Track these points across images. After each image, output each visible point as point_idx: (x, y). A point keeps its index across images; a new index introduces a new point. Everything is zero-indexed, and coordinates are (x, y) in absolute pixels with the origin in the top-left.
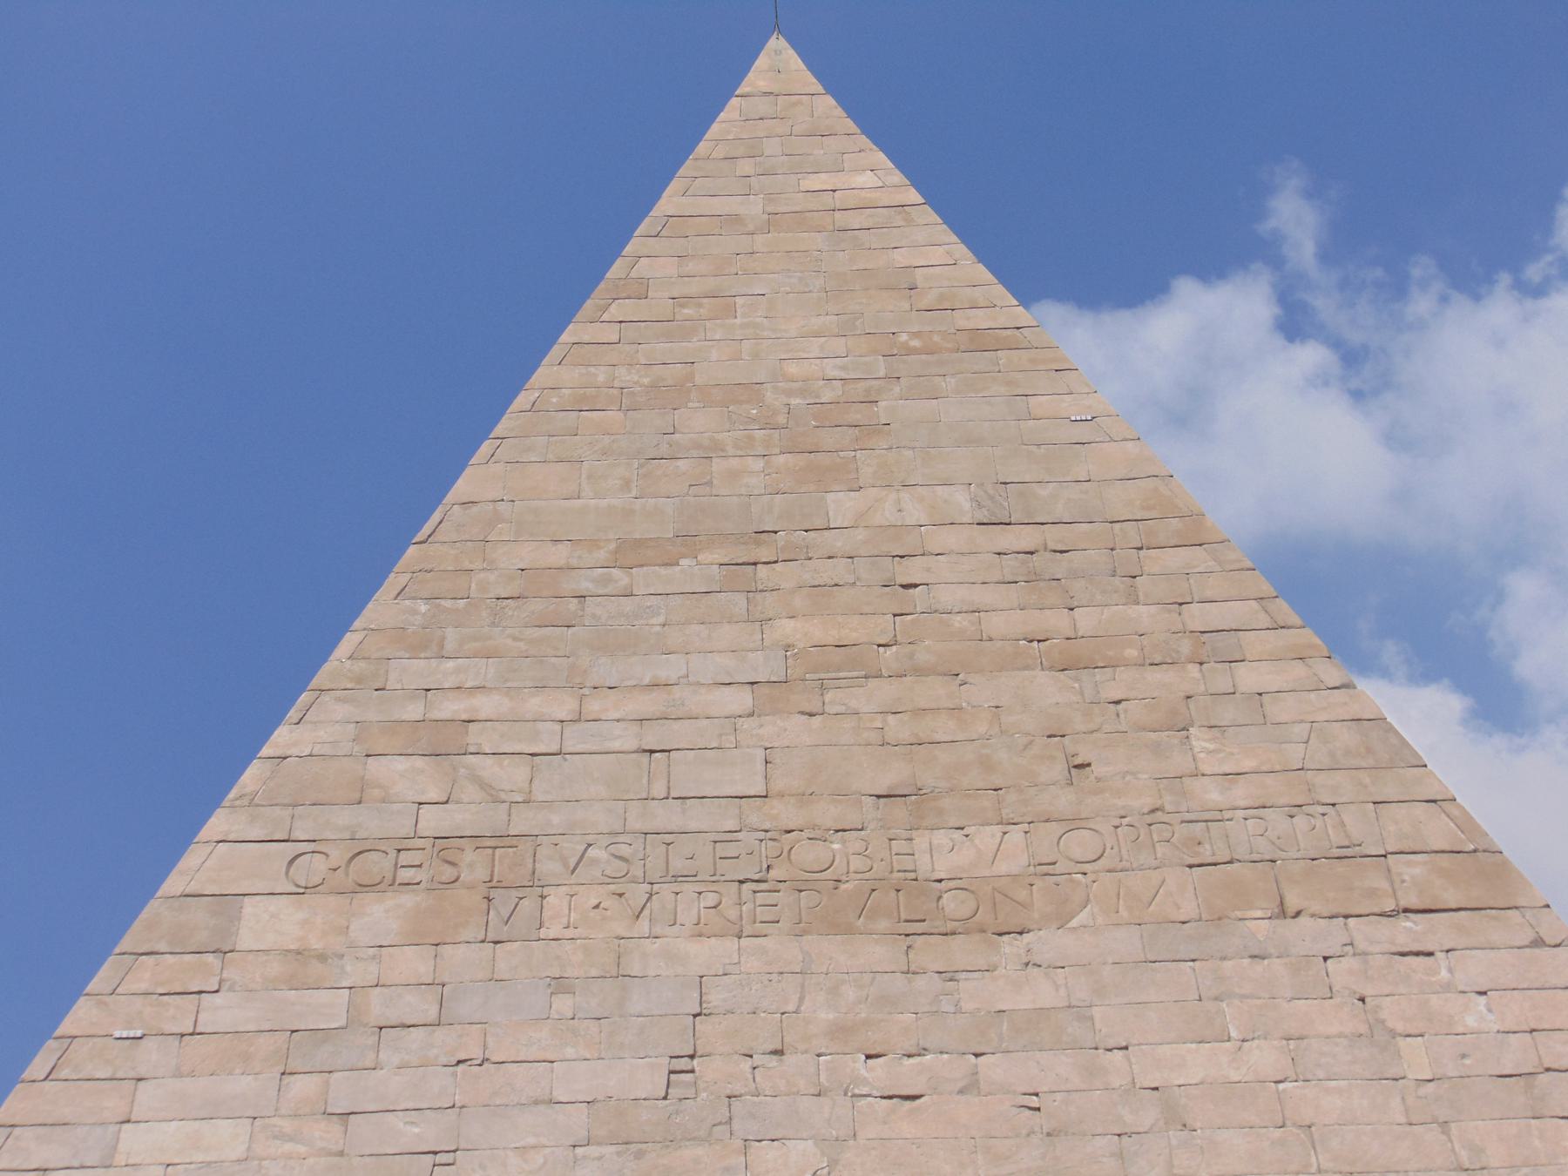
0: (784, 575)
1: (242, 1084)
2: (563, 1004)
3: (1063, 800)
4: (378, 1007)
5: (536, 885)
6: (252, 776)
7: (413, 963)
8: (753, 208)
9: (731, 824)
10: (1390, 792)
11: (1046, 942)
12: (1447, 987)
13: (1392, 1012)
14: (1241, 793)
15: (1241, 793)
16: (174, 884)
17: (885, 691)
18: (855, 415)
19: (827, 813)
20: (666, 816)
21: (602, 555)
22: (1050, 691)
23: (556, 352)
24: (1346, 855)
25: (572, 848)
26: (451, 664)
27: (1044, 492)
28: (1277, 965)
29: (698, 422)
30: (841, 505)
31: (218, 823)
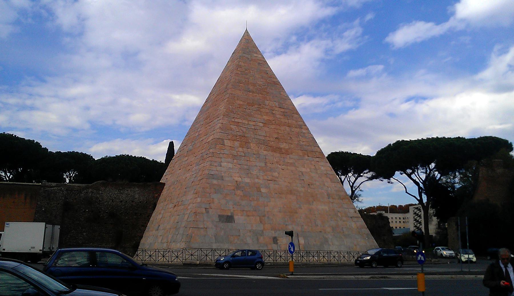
8: (249, 57)
11: (291, 156)
20: (258, 137)
22: (287, 129)
30: (267, 102)
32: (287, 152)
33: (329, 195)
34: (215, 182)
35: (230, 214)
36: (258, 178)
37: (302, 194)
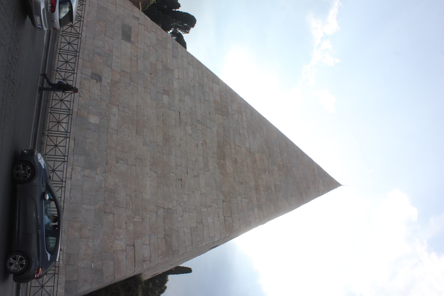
2: (208, 113)
22: (252, 184)
32: (222, 167)
35: (132, 39)
36: (181, 100)
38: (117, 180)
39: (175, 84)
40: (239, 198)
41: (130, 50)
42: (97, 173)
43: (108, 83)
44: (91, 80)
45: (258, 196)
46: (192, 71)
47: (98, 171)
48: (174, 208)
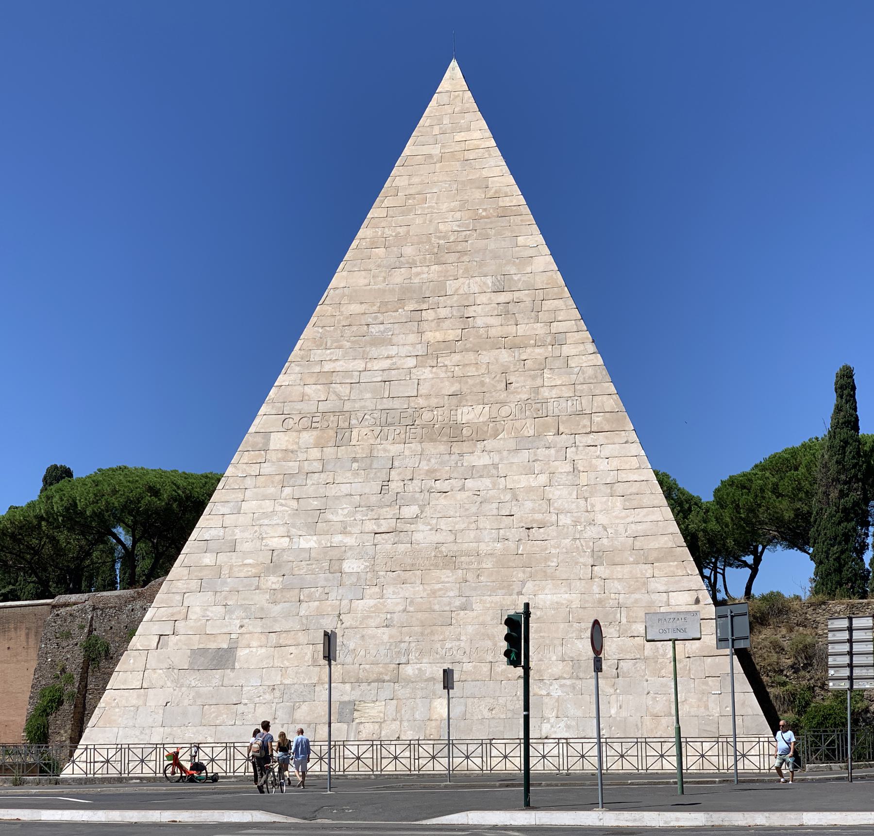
0: (429, 315)
1: (271, 490)
3: (503, 395)
4: (307, 467)
5: (350, 427)
6: (272, 393)
7: (315, 453)
8: (436, 151)
9: (406, 406)
10: (597, 392)
11: (489, 444)
12: (598, 457)
13: (580, 466)
14: (554, 393)
15: (554, 393)
16: (252, 429)
17: (456, 357)
18: (459, 248)
19: (434, 402)
21: (375, 308)
22: (505, 356)
23: (366, 222)
24: (581, 413)
25: (360, 415)
26: (329, 351)
27: (516, 278)
28: (552, 451)
29: (408, 250)
31: (263, 409)
32: (479, 436)
33: (598, 557)
34: (208, 559)
35: (225, 646)
36: (344, 532)
37: (488, 564)
38: (554, 658)
39: (307, 546)
40: (545, 393)
41: (254, 650)
42: (548, 694)
43: (353, 689)
44: (357, 721)
45: (532, 342)
46: (254, 502)
47: (544, 692)
48: (591, 544)
